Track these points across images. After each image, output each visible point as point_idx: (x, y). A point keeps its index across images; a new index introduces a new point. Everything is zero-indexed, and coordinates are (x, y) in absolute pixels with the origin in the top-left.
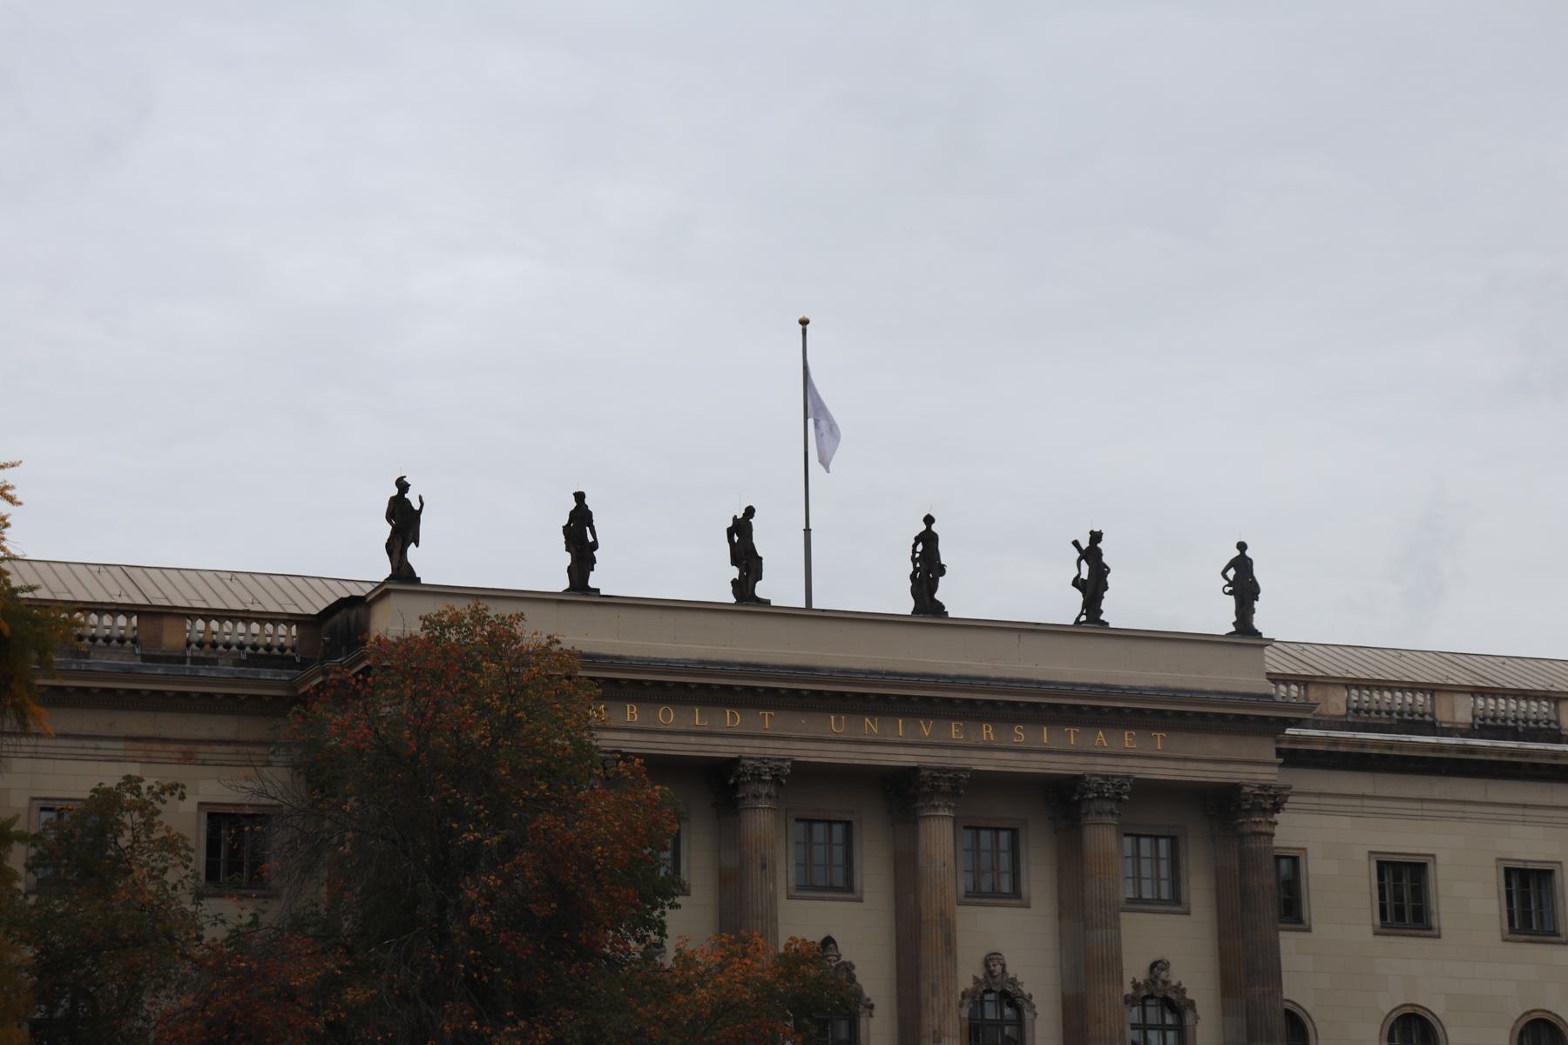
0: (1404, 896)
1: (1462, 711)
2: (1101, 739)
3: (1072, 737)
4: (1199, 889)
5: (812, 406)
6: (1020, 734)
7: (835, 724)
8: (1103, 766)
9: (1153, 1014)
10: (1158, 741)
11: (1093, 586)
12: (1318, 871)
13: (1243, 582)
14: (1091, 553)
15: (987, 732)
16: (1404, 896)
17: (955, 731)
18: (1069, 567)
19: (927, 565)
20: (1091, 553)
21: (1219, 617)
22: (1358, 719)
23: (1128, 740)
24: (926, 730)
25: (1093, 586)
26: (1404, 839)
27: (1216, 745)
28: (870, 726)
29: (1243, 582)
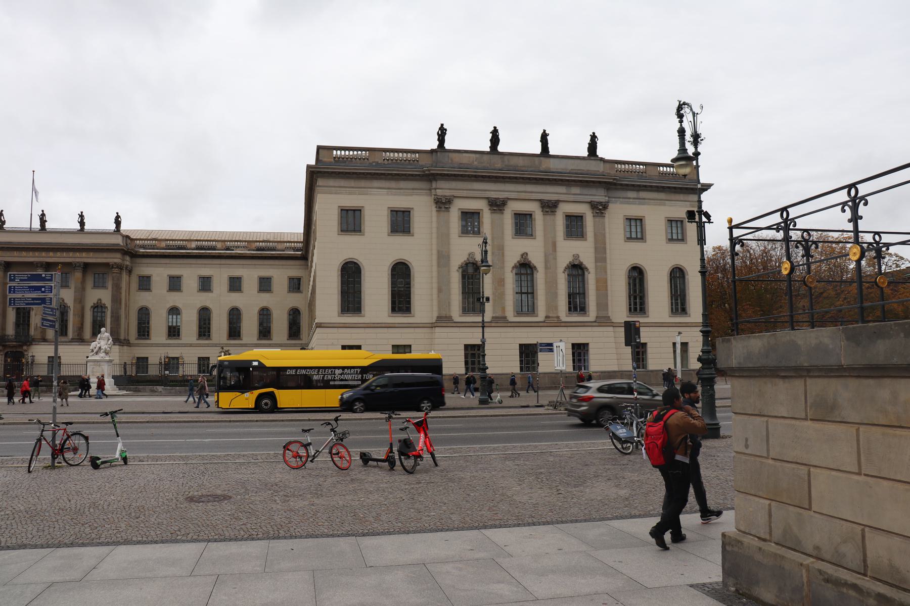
1: (194, 245)
2: (78, 254)
3: (71, 254)
4: (110, 284)
5: (34, 189)
6: (59, 254)
7: (15, 253)
8: (78, 260)
9: (100, 310)
10: (91, 254)
11: (82, 223)
12: (154, 279)
13: (118, 221)
14: (82, 216)
15: (51, 254)
17: (44, 254)
18: (77, 218)
19: (43, 221)
20: (82, 216)
21: (113, 227)
22: (168, 247)
23: (84, 254)
24: (37, 254)
25: (82, 223)
26: (175, 272)
27: (105, 255)
28: (24, 254)
29: (118, 221)
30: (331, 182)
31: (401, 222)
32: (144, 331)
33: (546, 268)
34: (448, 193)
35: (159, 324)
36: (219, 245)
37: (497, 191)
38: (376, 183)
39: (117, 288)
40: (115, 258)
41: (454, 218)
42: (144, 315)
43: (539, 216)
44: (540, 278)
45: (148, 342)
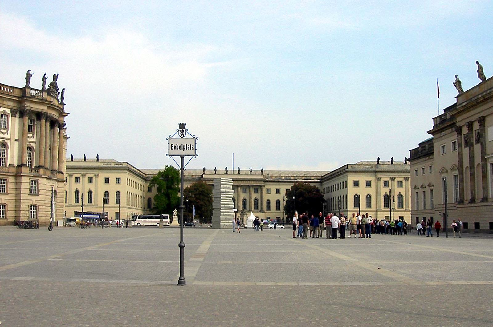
0: (278, 191)
8: (251, 184)
10: (255, 182)
16: (278, 191)
26: (278, 187)
30: (351, 174)
31: (368, 184)
32: (269, 208)
33: (406, 196)
34: (380, 176)
35: (273, 205)
36: (292, 178)
37: (392, 175)
38: (362, 174)
39: (262, 193)
40: (262, 184)
41: (382, 183)
42: (268, 203)
43: (404, 182)
44: (404, 198)
45: (270, 211)
